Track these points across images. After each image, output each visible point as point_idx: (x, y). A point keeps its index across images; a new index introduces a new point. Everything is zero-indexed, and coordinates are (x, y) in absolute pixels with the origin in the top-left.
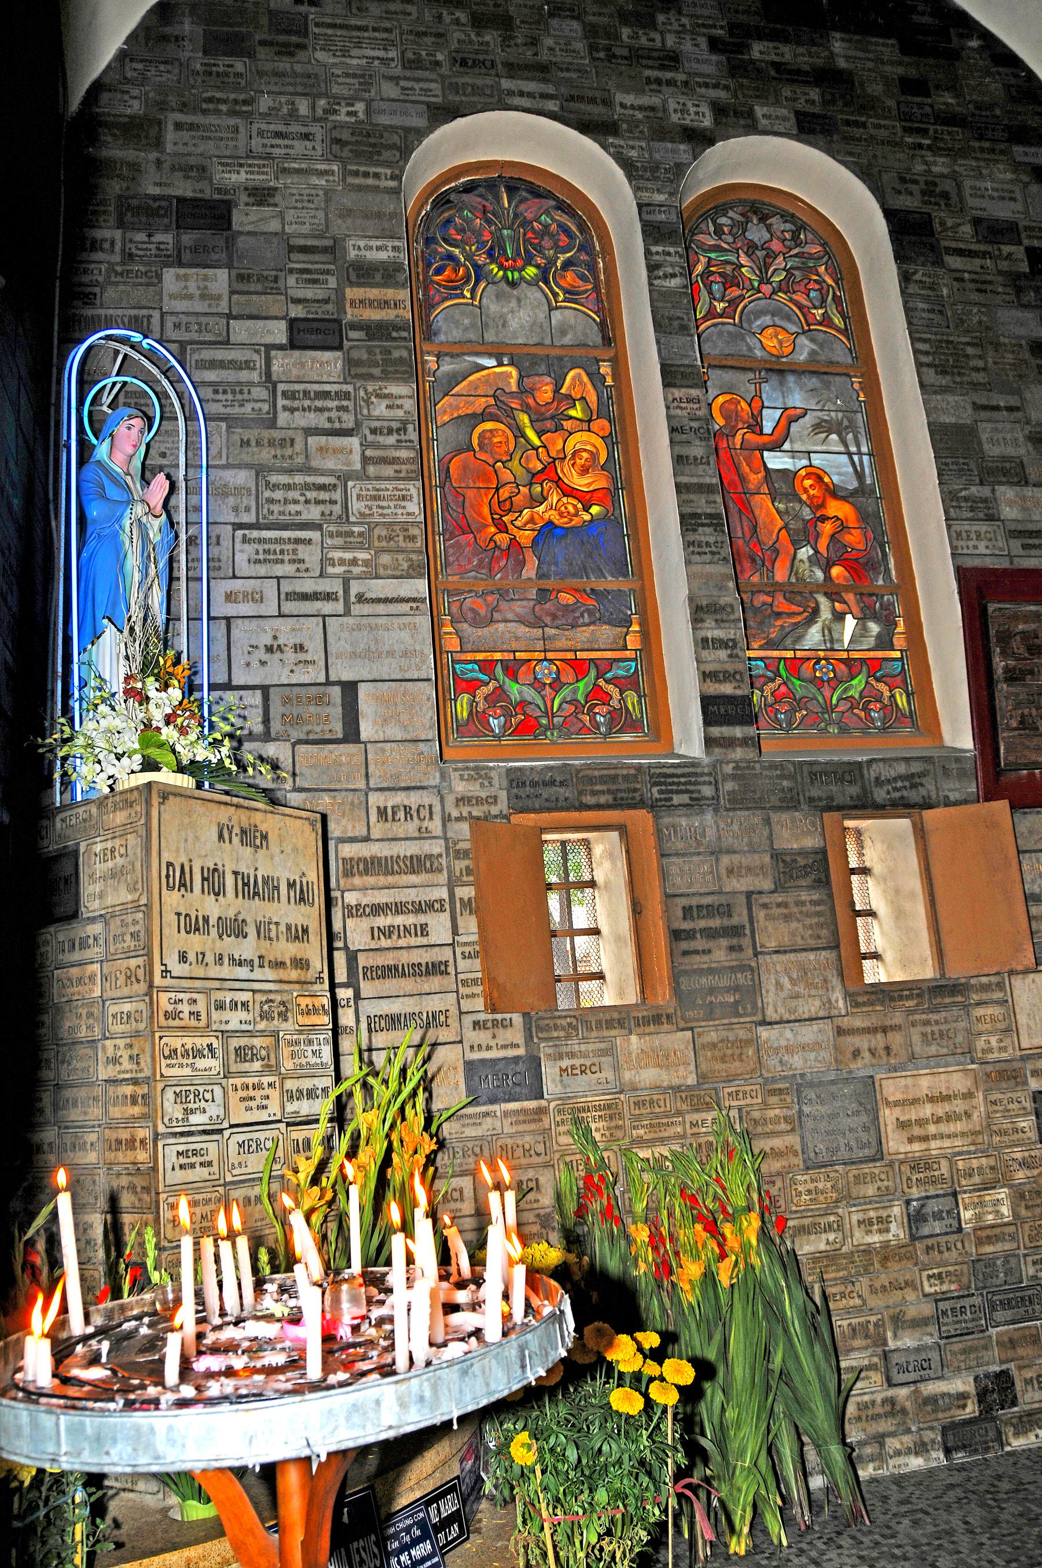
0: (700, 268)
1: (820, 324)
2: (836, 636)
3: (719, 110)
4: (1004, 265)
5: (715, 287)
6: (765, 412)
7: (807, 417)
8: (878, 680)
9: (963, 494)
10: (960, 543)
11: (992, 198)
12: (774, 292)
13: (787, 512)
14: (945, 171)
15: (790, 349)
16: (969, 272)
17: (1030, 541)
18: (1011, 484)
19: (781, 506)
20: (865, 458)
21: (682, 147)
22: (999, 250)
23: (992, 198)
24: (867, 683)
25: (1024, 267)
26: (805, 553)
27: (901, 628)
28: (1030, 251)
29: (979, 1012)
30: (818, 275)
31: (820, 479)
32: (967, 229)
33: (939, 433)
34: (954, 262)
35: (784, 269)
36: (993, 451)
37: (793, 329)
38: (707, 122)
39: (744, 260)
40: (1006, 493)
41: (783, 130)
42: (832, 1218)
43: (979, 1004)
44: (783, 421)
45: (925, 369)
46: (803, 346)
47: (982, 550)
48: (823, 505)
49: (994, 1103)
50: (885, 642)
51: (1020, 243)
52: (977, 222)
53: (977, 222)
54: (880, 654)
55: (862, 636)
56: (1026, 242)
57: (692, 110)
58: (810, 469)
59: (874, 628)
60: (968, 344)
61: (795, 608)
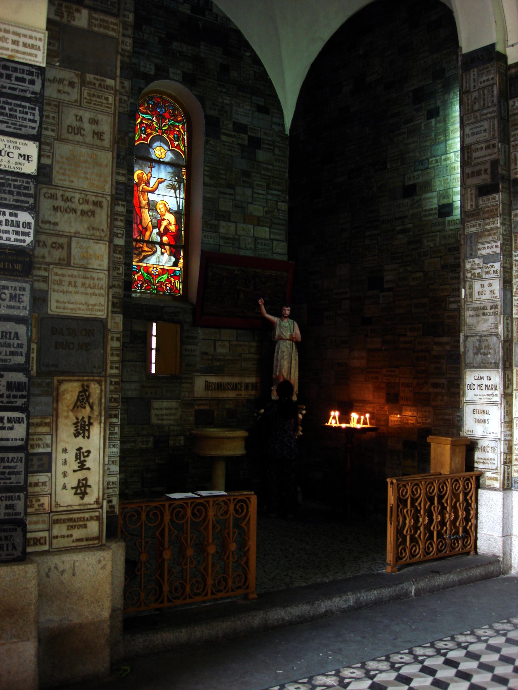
0: (139, 120)
1: (176, 147)
2: (160, 260)
3: (158, 68)
4: (240, 142)
5: (143, 129)
6: (151, 178)
7: (165, 182)
8: (171, 277)
9: (209, 222)
10: (205, 239)
11: (241, 115)
12: (163, 133)
13: (152, 216)
14: (228, 102)
15: (164, 156)
16: (228, 142)
17: (227, 241)
18: (224, 221)
19: (151, 214)
20: (181, 200)
21: (142, 81)
22: (240, 135)
23: (241, 115)
24: (168, 277)
25: (246, 143)
26: (156, 231)
27: (181, 260)
28: (250, 137)
29: (184, 385)
30: (179, 128)
31: (165, 205)
32: (231, 126)
33: (205, 200)
34: (224, 138)
35: (168, 125)
36: (222, 208)
37: (167, 148)
38: (152, 72)
39: (154, 119)
40: (223, 223)
41: (177, 79)
42: (133, 439)
43: (184, 383)
44: (157, 183)
45: (206, 177)
46: (169, 155)
47: (211, 242)
48: (164, 215)
49: (184, 412)
50: (175, 264)
51: (246, 133)
52: (235, 124)
53: (235, 124)
54: (174, 268)
55: (169, 261)
56: (249, 133)
57: (148, 66)
58: (163, 202)
59: (173, 259)
60: (222, 169)
61: (149, 250)
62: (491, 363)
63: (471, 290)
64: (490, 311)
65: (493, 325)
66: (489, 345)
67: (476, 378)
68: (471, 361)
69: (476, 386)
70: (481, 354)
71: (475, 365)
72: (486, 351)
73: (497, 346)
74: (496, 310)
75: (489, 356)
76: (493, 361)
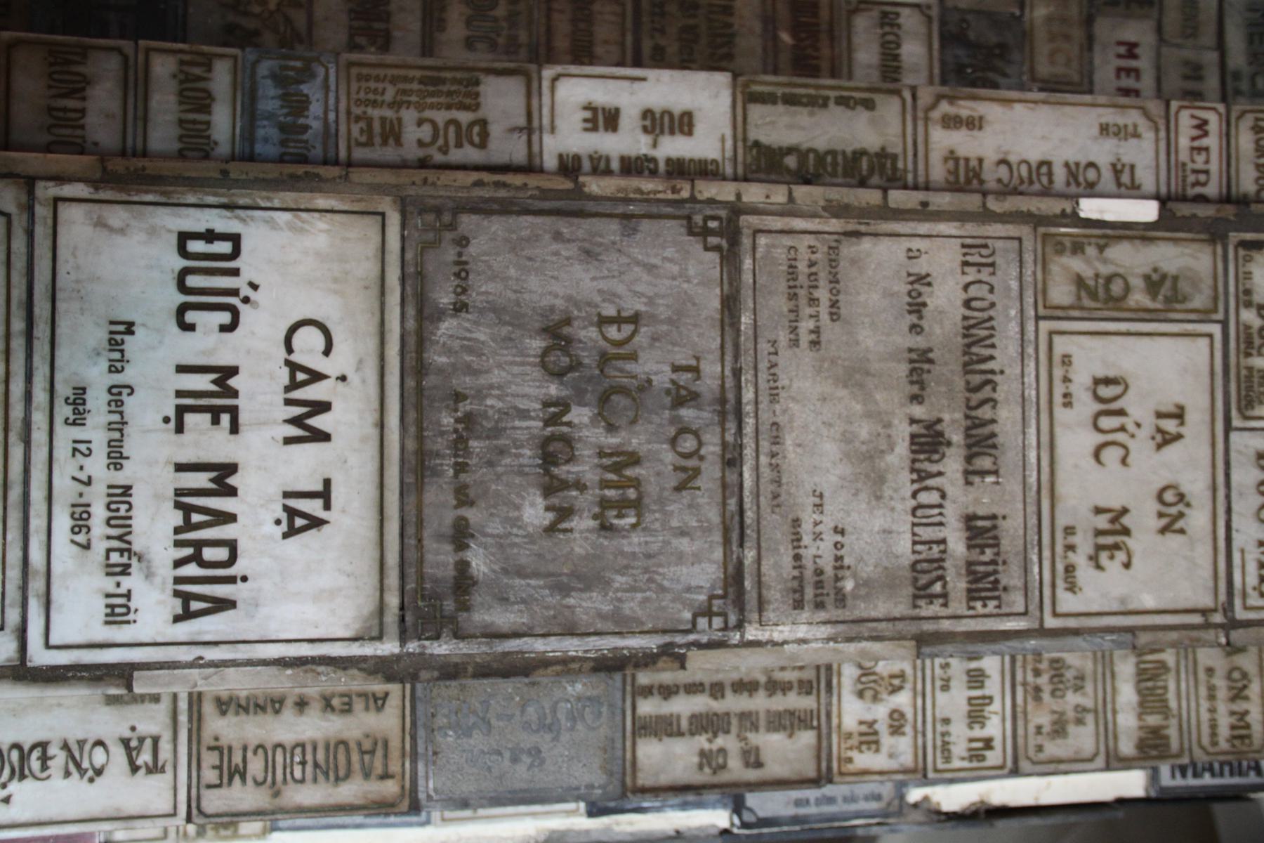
62: (461, 536)
63: (1139, 298)
64: (952, 515)
65: (825, 549)
66: (637, 505)
67: (308, 344)
68: (483, 289)
69: (224, 351)
70: (556, 411)
71: (447, 327)
72: (585, 468)
73: (631, 606)
74: (958, 584)
75: (535, 512)
76: (479, 562)
